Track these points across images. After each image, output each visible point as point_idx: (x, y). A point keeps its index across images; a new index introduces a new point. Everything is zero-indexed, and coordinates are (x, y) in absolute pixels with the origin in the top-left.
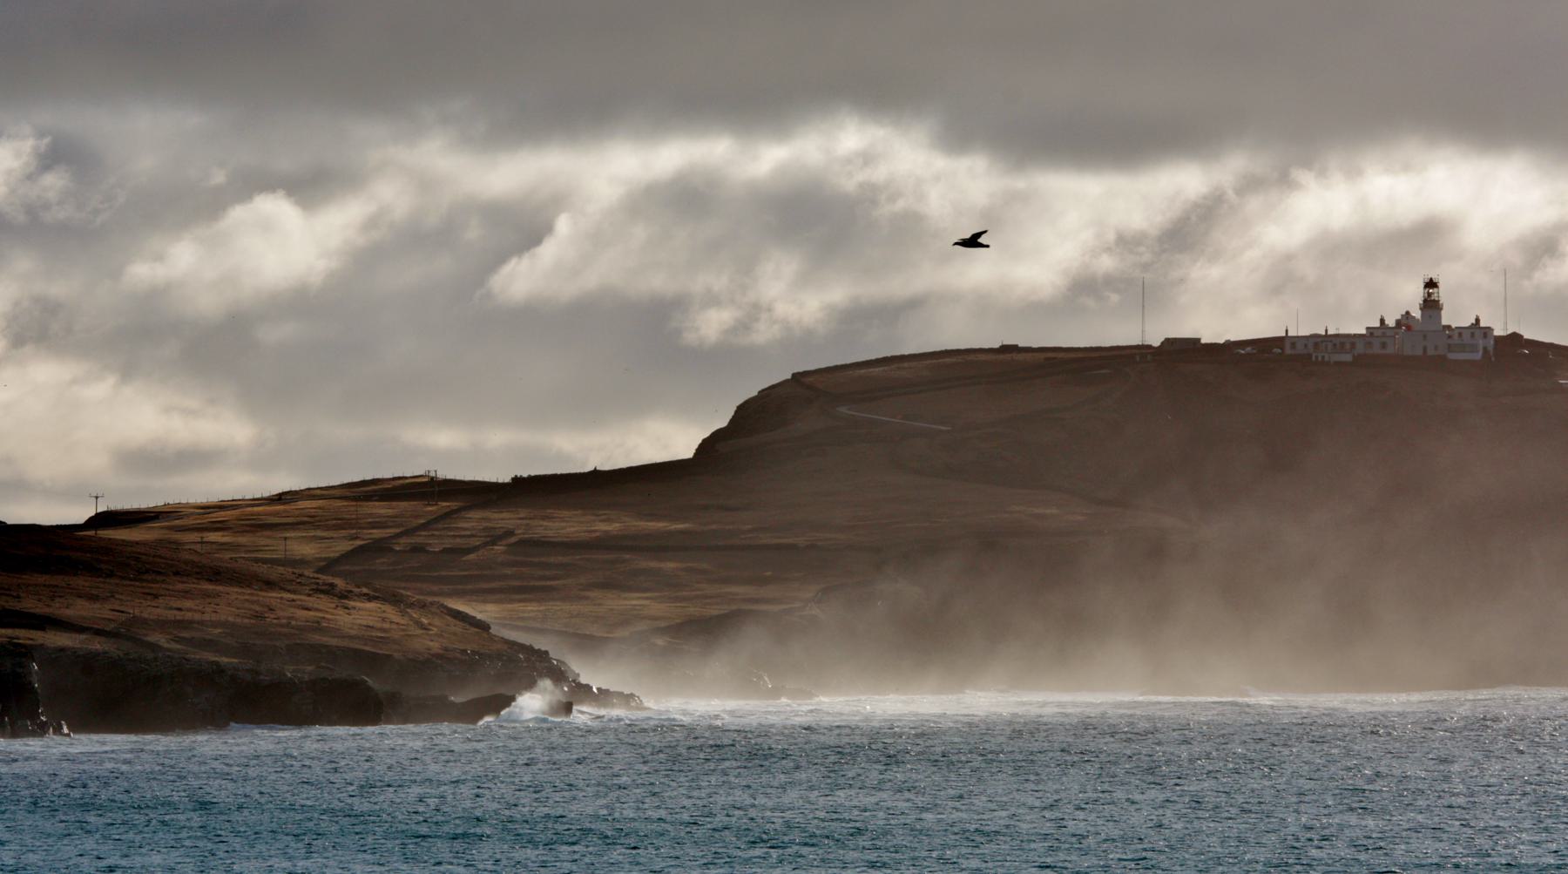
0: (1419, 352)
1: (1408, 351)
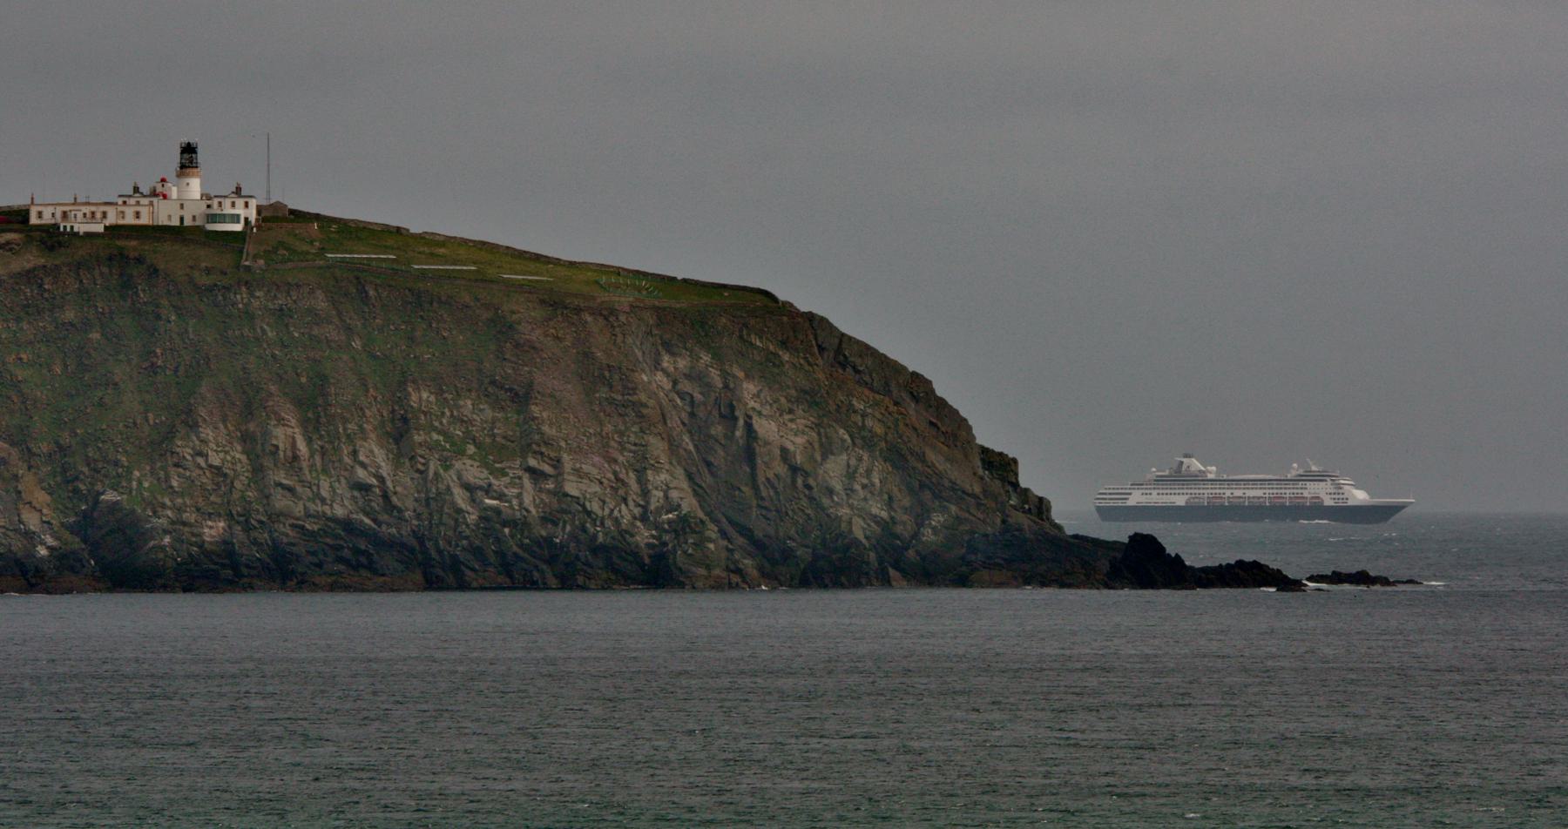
0: (177, 223)
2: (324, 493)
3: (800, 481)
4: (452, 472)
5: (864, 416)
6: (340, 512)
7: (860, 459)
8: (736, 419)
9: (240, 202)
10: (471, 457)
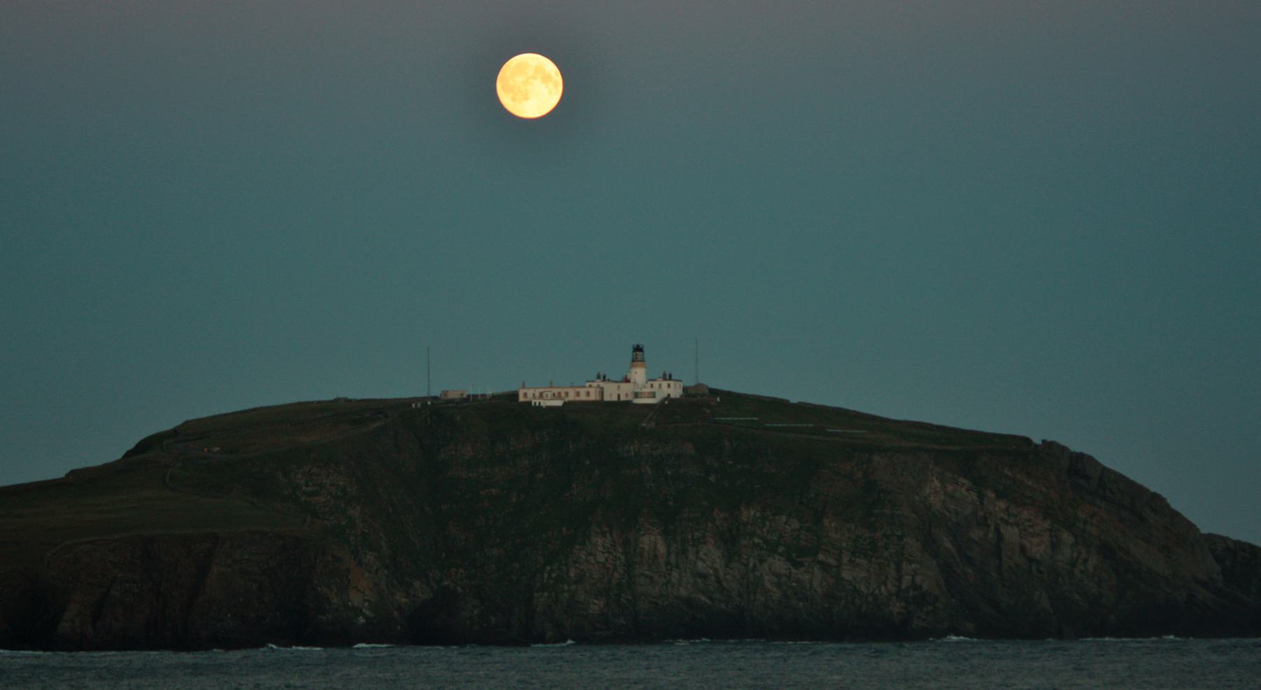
0: (615, 399)
1: (607, 398)
2: (674, 580)
3: (1034, 568)
4: (766, 565)
5: (1085, 523)
6: (683, 592)
7: (1080, 553)
8: (989, 526)
9: (665, 384)
10: (781, 555)
